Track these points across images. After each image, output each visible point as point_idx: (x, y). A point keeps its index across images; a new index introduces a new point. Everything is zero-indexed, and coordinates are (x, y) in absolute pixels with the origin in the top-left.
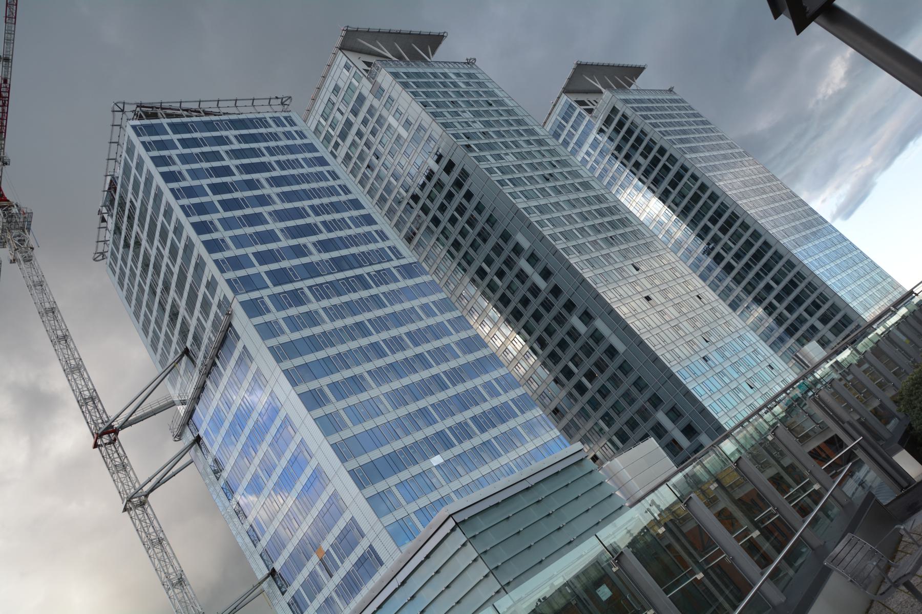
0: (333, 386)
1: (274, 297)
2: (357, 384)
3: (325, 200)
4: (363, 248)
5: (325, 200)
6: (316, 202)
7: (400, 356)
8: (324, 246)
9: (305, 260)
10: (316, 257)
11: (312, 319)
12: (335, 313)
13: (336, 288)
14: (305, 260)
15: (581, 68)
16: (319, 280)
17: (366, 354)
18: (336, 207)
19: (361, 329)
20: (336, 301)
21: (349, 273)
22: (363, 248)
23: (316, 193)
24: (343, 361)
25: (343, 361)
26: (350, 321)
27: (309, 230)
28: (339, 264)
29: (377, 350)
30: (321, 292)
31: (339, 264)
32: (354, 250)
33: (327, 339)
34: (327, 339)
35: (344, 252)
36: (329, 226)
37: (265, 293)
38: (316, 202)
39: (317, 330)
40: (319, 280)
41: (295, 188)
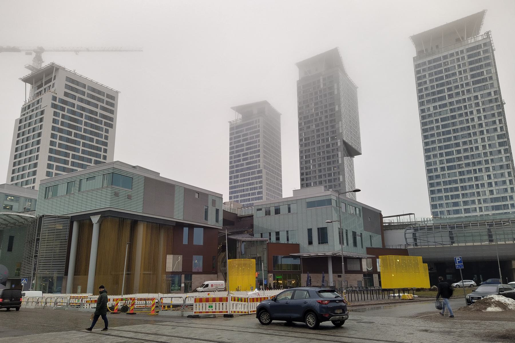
9: (242, 167)
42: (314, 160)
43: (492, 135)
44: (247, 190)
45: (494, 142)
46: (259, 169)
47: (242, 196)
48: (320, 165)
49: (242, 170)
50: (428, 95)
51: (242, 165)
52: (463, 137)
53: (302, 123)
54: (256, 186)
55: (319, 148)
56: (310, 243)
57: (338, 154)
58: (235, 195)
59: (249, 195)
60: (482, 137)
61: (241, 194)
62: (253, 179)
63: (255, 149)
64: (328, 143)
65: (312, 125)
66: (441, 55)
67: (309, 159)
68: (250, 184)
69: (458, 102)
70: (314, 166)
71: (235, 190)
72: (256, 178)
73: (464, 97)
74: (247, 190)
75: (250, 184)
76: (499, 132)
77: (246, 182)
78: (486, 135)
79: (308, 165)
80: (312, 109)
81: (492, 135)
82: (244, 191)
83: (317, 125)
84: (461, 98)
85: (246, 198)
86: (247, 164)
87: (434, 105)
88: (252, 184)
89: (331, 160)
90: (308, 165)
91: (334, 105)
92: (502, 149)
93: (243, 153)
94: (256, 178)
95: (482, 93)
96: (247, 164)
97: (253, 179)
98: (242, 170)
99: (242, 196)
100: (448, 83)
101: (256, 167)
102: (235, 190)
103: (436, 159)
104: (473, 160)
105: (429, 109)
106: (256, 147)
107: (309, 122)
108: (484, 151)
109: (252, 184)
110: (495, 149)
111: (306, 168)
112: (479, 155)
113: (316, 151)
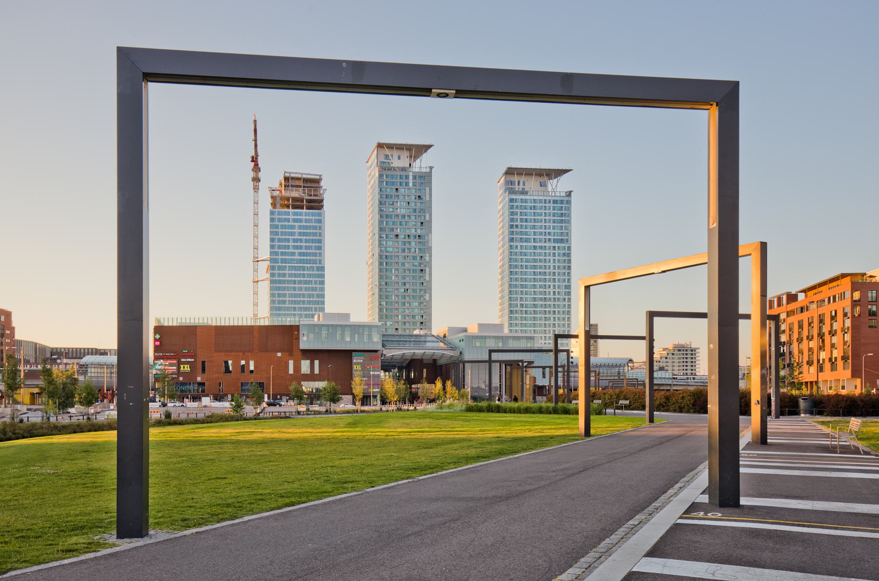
9: (293, 257)
12: (291, 275)
13: (295, 268)
15: (510, 172)
18: (313, 241)
19: (295, 282)
21: (302, 265)
24: (284, 289)
25: (284, 289)
26: (293, 279)
28: (300, 261)
29: (294, 289)
30: (291, 268)
31: (300, 261)
33: (284, 282)
34: (284, 282)
36: (307, 248)
43: (562, 284)
44: (300, 289)
45: (562, 290)
46: (320, 265)
47: (292, 295)
48: (404, 278)
49: (290, 261)
51: (293, 254)
52: (540, 280)
56: (544, 377)
57: (425, 270)
59: (304, 296)
60: (554, 284)
62: (309, 276)
63: (314, 238)
64: (414, 255)
65: (397, 229)
67: (391, 267)
68: (306, 282)
69: (541, 247)
70: (397, 276)
73: (545, 244)
74: (300, 289)
75: (306, 282)
76: (566, 284)
77: (299, 279)
78: (557, 284)
80: (397, 209)
81: (562, 284)
82: (294, 289)
84: (543, 245)
86: (300, 254)
87: (521, 244)
88: (309, 282)
91: (424, 212)
92: (567, 297)
93: (293, 237)
95: (559, 245)
96: (300, 254)
97: (309, 276)
98: (290, 261)
99: (292, 295)
101: (315, 262)
103: (518, 296)
104: (545, 303)
105: (517, 247)
106: (315, 234)
108: (554, 297)
109: (309, 282)
110: (561, 297)
112: (550, 300)
113: (401, 260)
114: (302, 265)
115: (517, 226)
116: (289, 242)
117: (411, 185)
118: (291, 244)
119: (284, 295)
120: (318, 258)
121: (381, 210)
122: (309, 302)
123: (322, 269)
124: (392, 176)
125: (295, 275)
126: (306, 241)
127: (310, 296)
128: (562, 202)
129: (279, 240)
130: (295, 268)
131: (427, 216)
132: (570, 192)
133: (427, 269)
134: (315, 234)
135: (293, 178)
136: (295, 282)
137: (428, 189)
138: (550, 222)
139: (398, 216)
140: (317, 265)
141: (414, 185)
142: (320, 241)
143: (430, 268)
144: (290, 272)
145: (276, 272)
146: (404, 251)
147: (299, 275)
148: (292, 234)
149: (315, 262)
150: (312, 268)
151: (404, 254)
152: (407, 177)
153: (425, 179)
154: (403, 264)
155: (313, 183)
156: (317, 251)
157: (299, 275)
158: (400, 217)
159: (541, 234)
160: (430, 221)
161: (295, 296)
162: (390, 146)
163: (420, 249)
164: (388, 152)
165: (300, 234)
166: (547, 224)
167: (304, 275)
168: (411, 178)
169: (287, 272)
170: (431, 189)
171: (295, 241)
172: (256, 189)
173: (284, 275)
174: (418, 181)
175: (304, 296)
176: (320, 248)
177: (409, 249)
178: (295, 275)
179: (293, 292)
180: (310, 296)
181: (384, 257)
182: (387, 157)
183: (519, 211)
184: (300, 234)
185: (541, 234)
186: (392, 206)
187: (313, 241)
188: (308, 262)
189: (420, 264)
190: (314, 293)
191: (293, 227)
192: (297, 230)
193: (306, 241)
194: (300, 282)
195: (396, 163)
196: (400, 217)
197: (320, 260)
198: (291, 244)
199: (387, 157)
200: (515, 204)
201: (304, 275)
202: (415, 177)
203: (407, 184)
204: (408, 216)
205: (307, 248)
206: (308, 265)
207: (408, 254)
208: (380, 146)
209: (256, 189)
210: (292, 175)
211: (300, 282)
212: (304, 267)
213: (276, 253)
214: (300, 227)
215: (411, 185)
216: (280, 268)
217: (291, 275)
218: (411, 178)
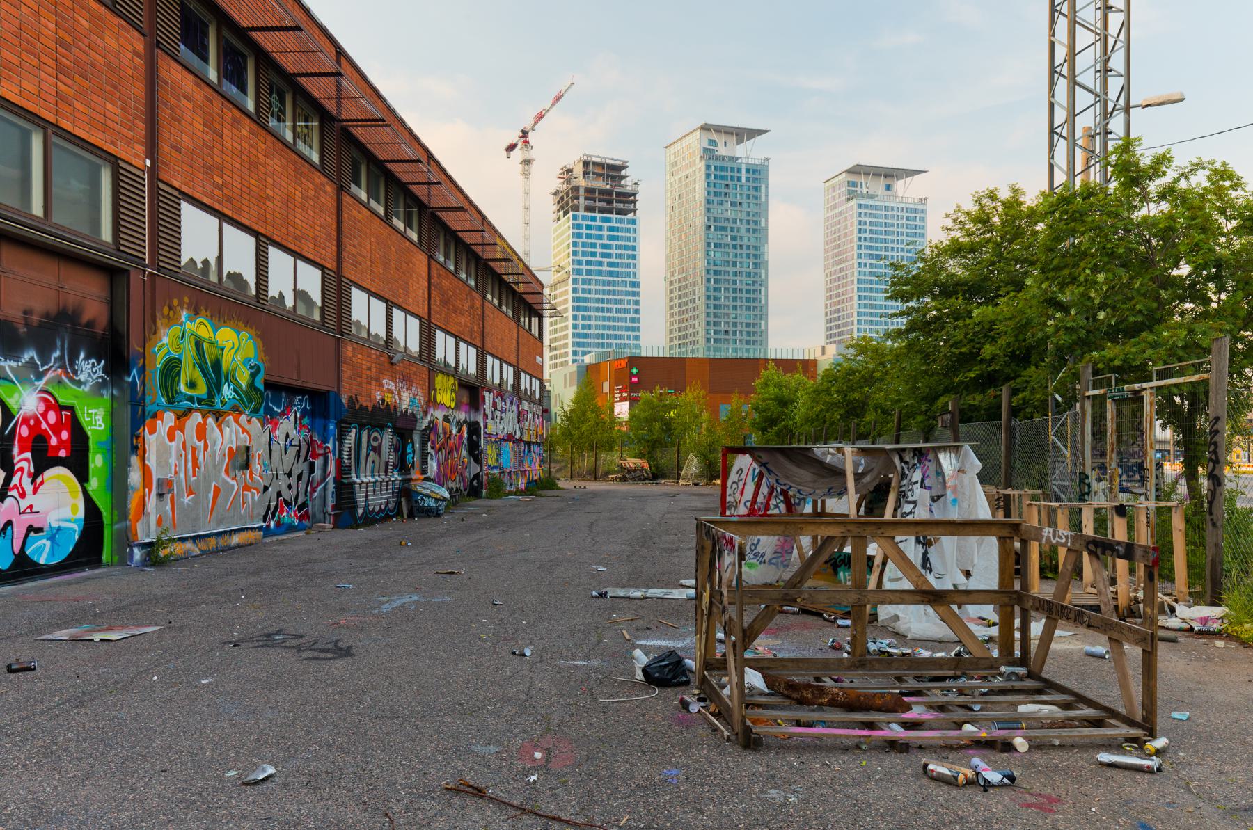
0: (583, 316)
1: (583, 280)
2: (589, 318)
3: (623, 243)
4: (624, 270)
5: (623, 243)
6: (619, 243)
7: (608, 314)
8: (611, 265)
9: (600, 268)
10: (605, 268)
11: (589, 291)
12: (598, 292)
13: (604, 283)
14: (600, 268)
15: (855, 171)
16: (601, 278)
17: (597, 310)
18: (626, 248)
19: (602, 301)
20: (601, 288)
21: (612, 279)
22: (624, 270)
23: (622, 239)
24: (590, 309)
25: (590, 309)
26: (601, 296)
27: (609, 255)
28: (611, 274)
29: (602, 310)
30: (599, 282)
31: (611, 274)
32: (620, 269)
35: (616, 269)
36: (618, 256)
37: (581, 277)
38: (619, 243)
39: (589, 296)
40: (601, 278)
41: (616, 234)
42: (727, 289)
44: (610, 310)
47: (599, 318)
50: (866, 247)
51: (600, 264)
53: (710, 227)
54: (626, 306)
55: (735, 274)
58: (585, 314)
59: (614, 319)
61: (597, 314)
62: (621, 293)
64: (748, 270)
66: (882, 204)
68: (616, 302)
70: (727, 298)
71: (585, 305)
72: (627, 293)
74: (610, 310)
75: (616, 302)
79: (717, 294)
82: (602, 310)
83: (734, 238)
85: (608, 323)
86: (611, 265)
89: (752, 296)
90: (717, 294)
94: (627, 293)
97: (621, 293)
99: (599, 318)
100: (885, 241)
101: (628, 275)
102: (585, 305)
106: (628, 239)
107: (722, 229)
111: (715, 299)
113: (731, 277)
114: (612, 279)
115: (866, 239)
116: (595, 247)
117: (743, 180)
118: (599, 250)
119: (589, 318)
120: (631, 270)
121: (708, 210)
122: (621, 328)
123: (635, 284)
124: (722, 169)
125: (604, 292)
126: (618, 247)
127: (621, 320)
128: (916, 211)
129: (584, 245)
130: (604, 283)
131: (763, 220)
132: (926, 199)
133: (763, 289)
134: (628, 239)
135: (595, 164)
136: (602, 301)
137: (763, 187)
138: (902, 235)
139: (728, 219)
140: (631, 280)
141: (748, 180)
142: (634, 248)
143: (767, 288)
144: (597, 287)
145: (580, 286)
146: (735, 264)
147: (609, 292)
148: (600, 237)
149: (628, 275)
150: (624, 284)
151: (735, 269)
152: (739, 170)
153: (758, 174)
154: (734, 282)
155: (614, 171)
156: (630, 261)
157: (609, 292)
158: (731, 221)
159: (893, 249)
160: (766, 229)
161: (604, 319)
162: (718, 129)
163: (753, 263)
164: (714, 136)
165: (610, 238)
166: (900, 238)
167: (614, 293)
168: (744, 171)
169: (593, 287)
170: (767, 187)
171: (604, 246)
172: (526, 174)
173: (589, 291)
174: (751, 176)
175: (614, 319)
176: (634, 257)
177: (740, 262)
178: (604, 292)
179: (601, 314)
180: (621, 320)
181: (712, 272)
182: (713, 142)
183: (868, 220)
184: (610, 238)
185: (893, 249)
186: (721, 207)
187: (626, 248)
188: (619, 274)
189: (754, 282)
190: (627, 315)
191: (600, 228)
192: (606, 233)
193: (618, 247)
194: (610, 301)
195: (721, 151)
196: (731, 221)
197: (634, 274)
198: (599, 250)
199: (713, 142)
200: (864, 211)
201: (614, 293)
202: (748, 171)
203: (739, 179)
204: (741, 220)
205: (618, 256)
206: (620, 279)
207: (741, 270)
208: (705, 128)
209: (526, 174)
210: (594, 159)
211: (610, 301)
212: (614, 281)
213: (579, 262)
214: (611, 229)
215: (743, 180)
216: (584, 282)
217: (598, 292)
218: (744, 171)
